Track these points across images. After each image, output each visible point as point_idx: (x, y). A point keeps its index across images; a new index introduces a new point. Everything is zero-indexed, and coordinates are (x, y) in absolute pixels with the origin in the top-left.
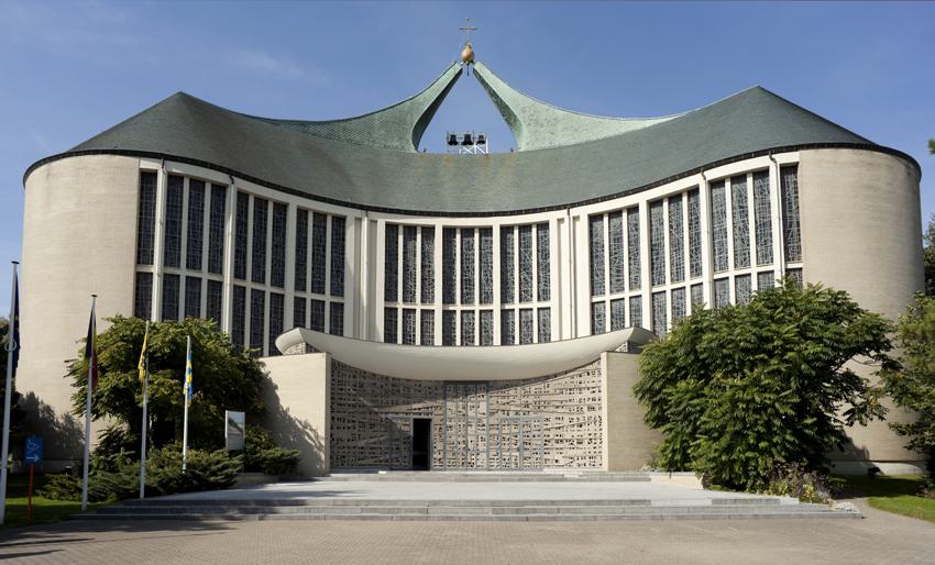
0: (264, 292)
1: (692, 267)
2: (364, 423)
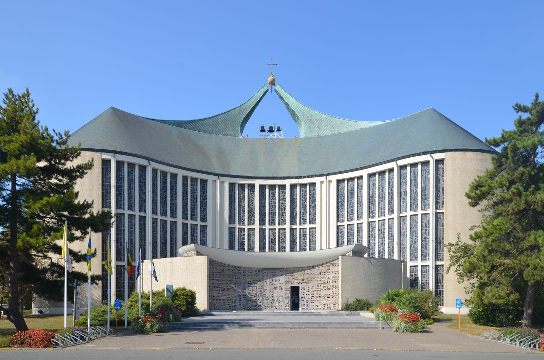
0: (166, 221)
1: (389, 209)
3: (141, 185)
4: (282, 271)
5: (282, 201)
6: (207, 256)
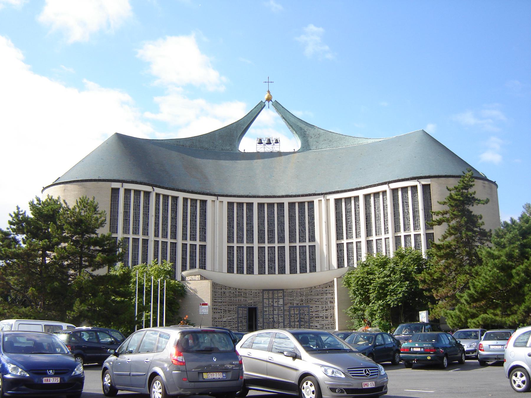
2: (226, 310)
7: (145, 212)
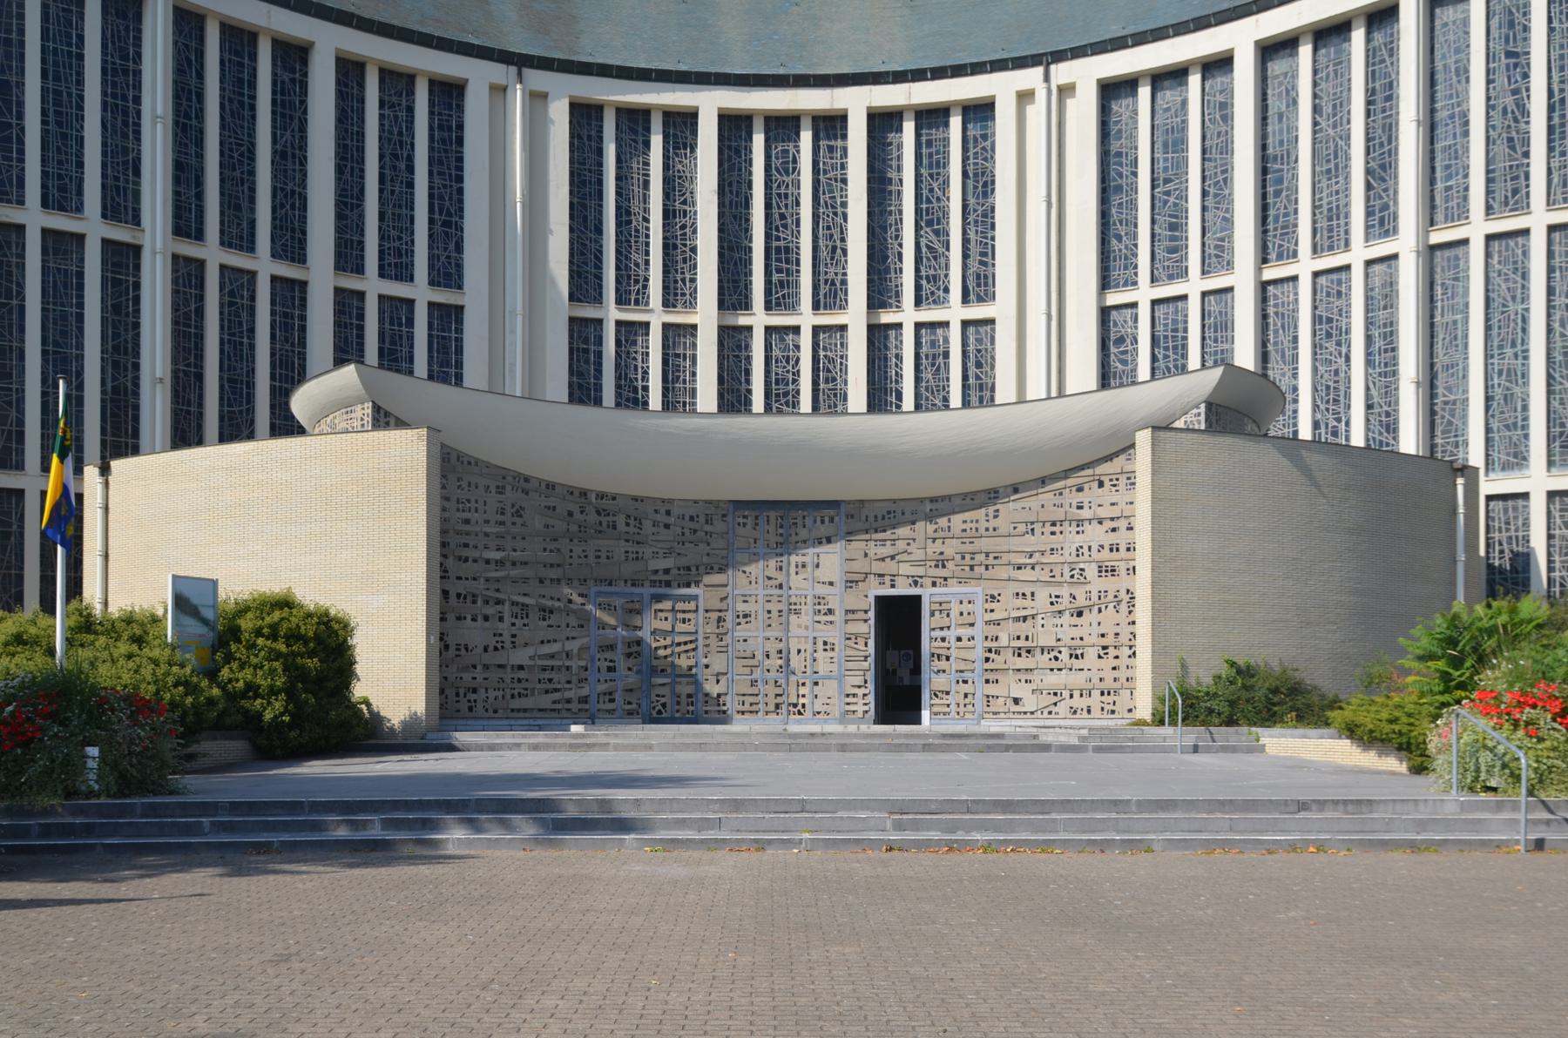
1: (1369, 213)
3: (114, 84)
4: (832, 520)
5: (831, 191)
6: (424, 432)
7: (114, 96)
